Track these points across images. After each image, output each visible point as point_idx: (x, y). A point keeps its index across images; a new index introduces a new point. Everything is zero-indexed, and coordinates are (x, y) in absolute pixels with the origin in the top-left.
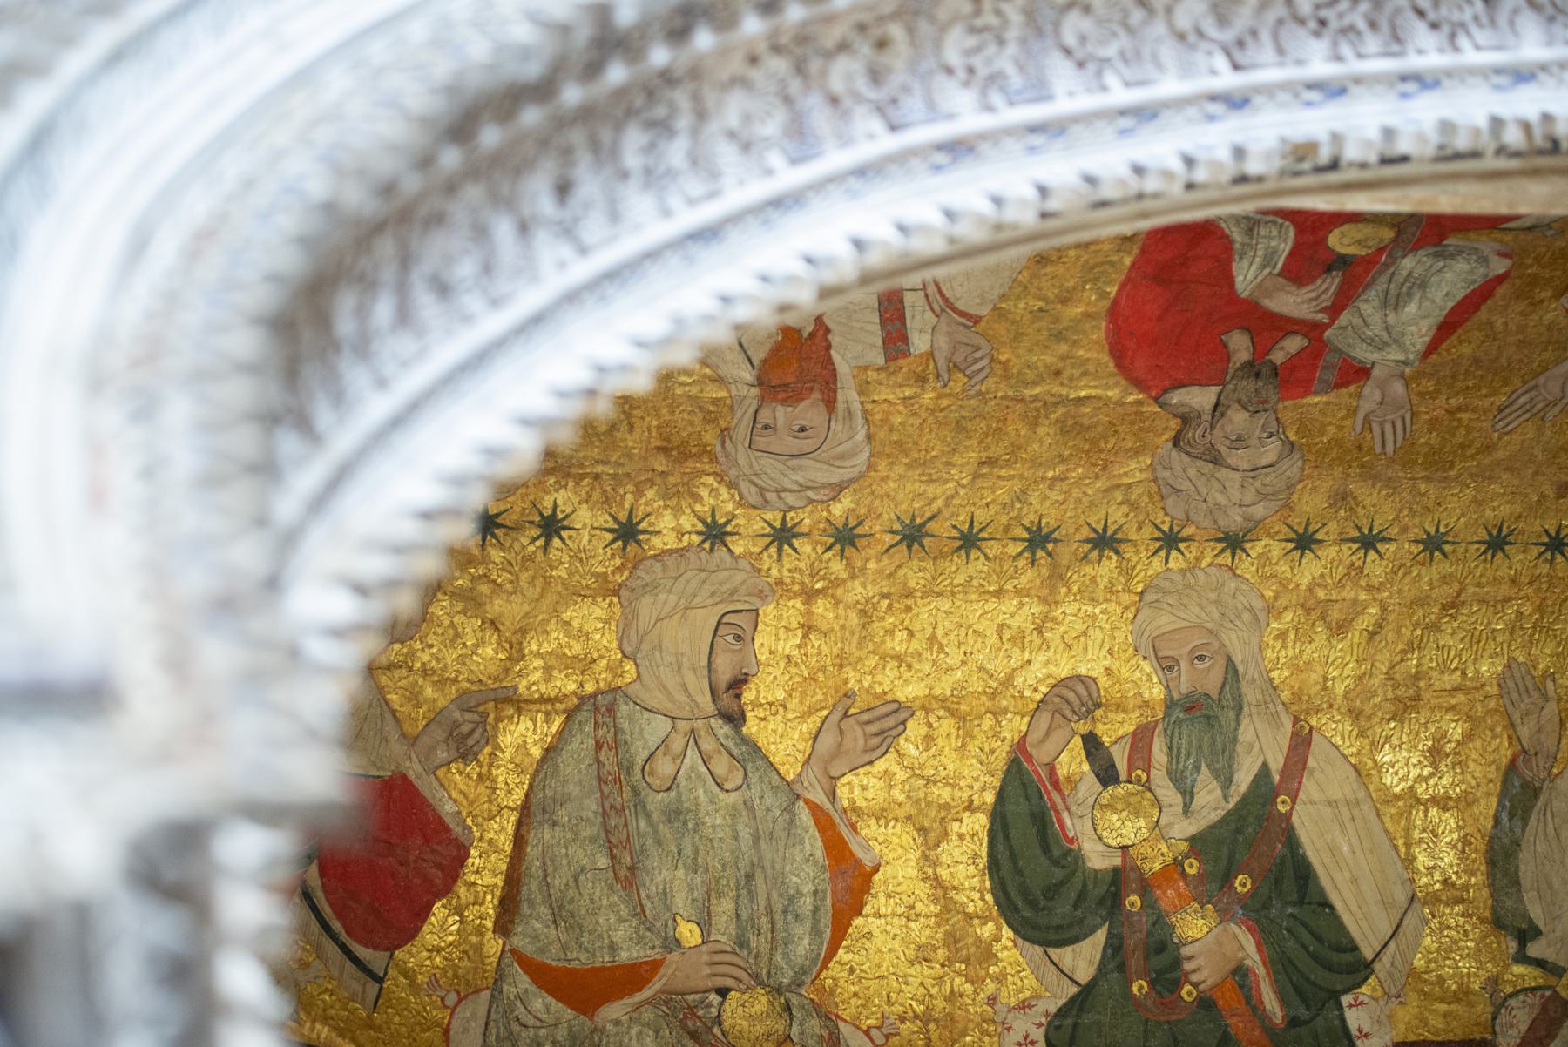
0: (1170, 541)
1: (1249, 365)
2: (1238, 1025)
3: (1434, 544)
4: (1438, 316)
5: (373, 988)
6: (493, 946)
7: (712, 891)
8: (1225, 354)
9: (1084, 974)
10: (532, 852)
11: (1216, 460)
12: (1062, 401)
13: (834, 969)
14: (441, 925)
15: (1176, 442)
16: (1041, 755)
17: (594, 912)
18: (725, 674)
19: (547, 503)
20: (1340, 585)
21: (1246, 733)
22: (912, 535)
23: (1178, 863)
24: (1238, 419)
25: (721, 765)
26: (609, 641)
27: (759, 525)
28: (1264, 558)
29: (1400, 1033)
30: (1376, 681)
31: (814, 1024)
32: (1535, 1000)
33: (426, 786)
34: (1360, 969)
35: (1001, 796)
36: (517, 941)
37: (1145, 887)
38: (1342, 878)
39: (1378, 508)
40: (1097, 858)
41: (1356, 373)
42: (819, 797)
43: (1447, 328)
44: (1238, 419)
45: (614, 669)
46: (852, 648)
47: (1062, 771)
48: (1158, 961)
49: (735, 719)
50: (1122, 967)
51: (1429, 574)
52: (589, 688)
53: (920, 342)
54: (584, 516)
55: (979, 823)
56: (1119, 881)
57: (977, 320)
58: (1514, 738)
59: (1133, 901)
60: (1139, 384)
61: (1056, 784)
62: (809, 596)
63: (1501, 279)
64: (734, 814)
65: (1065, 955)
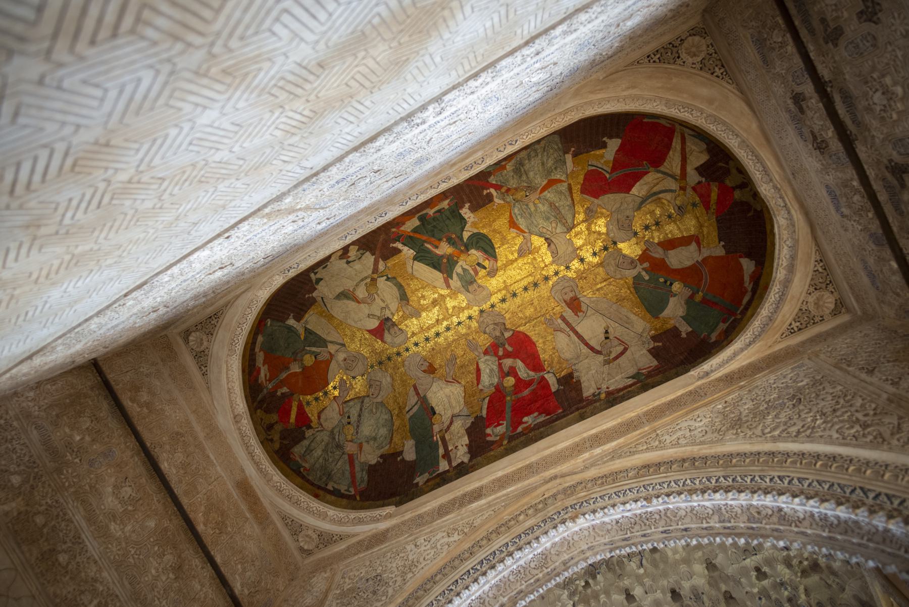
0: (493, 306)
1: (504, 345)
2: (433, 239)
3: (448, 329)
4: (482, 372)
5: (590, 163)
6: (571, 181)
7: (536, 210)
8: (509, 344)
9: (464, 233)
10: (570, 199)
11: (495, 324)
12: (529, 322)
13: (509, 210)
14: (581, 178)
15: (504, 324)
16: (492, 262)
17: (555, 196)
18: (552, 245)
19: (598, 258)
20: (459, 314)
21: (459, 283)
22: (536, 285)
23: (458, 258)
24: (498, 334)
25: (544, 230)
26: (575, 240)
27: (562, 273)
28: (475, 311)
29: (402, 254)
30: (442, 303)
31: (508, 200)
32: (380, 271)
33: (593, 199)
34: (415, 258)
35: (495, 251)
36: (565, 184)
37: (462, 251)
38: (427, 270)
39: (463, 330)
40: (473, 251)
41: (486, 353)
42: (525, 235)
43: (478, 370)
44: (498, 334)
45: (570, 235)
46: (534, 262)
47: (487, 261)
48: (452, 242)
49: (546, 239)
50: (458, 237)
51: (445, 323)
52: (573, 230)
53: (560, 321)
54: (591, 259)
55: (496, 246)
56: (467, 249)
57: (554, 331)
58: (411, 306)
59: (463, 248)
60: (519, 332)
61: (487, 259)
62: (546, 266)
63: (478, 384)
64: (539, 225)
65: (469, 234)
